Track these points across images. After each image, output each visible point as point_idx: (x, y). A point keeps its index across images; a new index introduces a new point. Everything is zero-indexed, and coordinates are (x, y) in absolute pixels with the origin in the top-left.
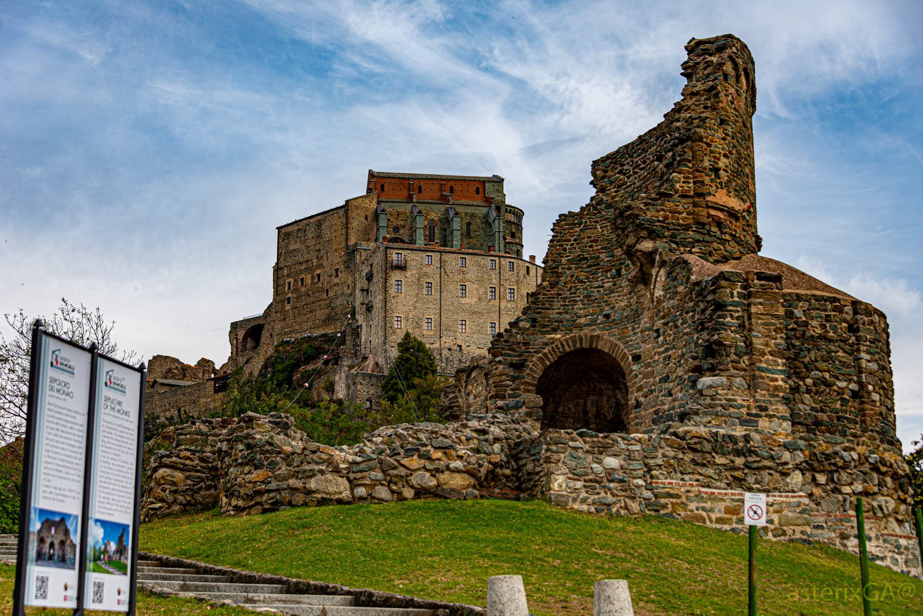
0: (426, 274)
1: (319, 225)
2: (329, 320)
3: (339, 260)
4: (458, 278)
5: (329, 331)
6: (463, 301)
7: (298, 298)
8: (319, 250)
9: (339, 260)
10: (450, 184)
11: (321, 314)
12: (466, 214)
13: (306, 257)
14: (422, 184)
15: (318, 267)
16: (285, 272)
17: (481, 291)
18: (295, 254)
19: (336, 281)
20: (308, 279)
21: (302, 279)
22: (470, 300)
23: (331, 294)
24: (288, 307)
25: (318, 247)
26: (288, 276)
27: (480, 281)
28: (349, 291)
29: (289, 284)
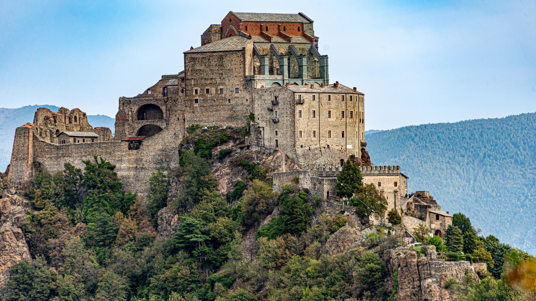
0: (313, 106)
1: (221, 58)
2: (231, 118)
3: (238, 83)
4: (327, 107)
5: (233, 125)
6: (330, 120)
7: (205, 100)
8: (222, 74)
9: (238, 83)
10: (284, 25)
11: (224, 113)
12: (300, 49)
13: (211, 76)
14: (268, 25)
15: (223, 84)
16: (193, 82)
17: (338, 114)
18: (201, 72)
19: (237, 95)
20: (213, 90)
21: (208, 91)
22: (333, 119)
23: (232, 102)
24: (196, 105)
25: (221, 72)
27: (337, 108)
28: (248, 103)
29: (196, 91)
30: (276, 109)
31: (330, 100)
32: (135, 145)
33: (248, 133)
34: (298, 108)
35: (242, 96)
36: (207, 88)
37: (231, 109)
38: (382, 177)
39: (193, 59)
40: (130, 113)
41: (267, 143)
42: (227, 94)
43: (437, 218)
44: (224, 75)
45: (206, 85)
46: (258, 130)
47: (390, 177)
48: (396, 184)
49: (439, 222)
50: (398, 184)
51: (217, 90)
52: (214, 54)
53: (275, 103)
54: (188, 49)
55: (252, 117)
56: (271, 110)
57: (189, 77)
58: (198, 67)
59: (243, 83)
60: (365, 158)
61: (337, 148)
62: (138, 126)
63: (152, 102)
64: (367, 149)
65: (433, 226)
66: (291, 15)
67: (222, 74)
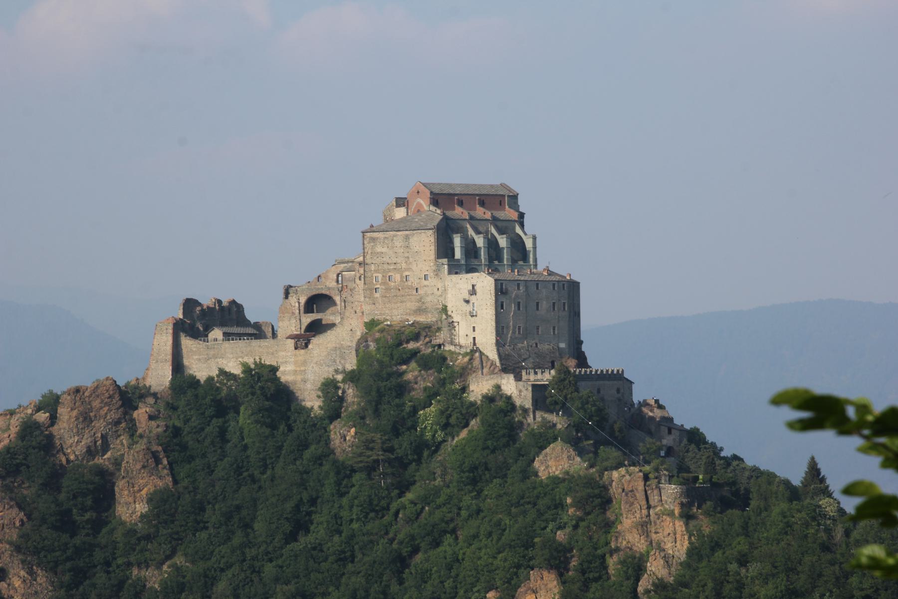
1: (407, 238)
2: (420, 311)
5: (422, 319)
6: (538, 313)
7: (388, 289)
8: (408, 257)
11: (412, 305)
13: (394, 260)
14: (463, 198)
15: (409, 269)
16: (373, 267)
19: (426, 283)
20: (397, 277)
23: (420, 292)
25: (407, 255)
26: (376, 271)
28: (439, 293)
30: (473, 299)
31: (537, 288)
32: (302, 341)
33: (439, 329)
34: (502, 298)
35: (432, 284)
36: (390, 274)
37: (420, 300)
38: (601, 382)
39: (373, 240)
40: (297, 305)
41: (462, 341)
42: (413, 281)
43: (670, 432)
44: (411, 259)
45: (389, 270)
46: (452, 326)
47: (611, 383)
48: (618, 391)
49: (671, 437)
50: (622, 391)
51: (402, 277)
52: (399, 233)
53: (473, 292)
54: (367, 227)
55: (445, 309)
56: (467, 302)
57: (368, 261)
58: (379, 249)
59: (434, 268)
60: (582, 361)
61: (547, 347)
62: (307, 319)
63: (324, 292)
64: (584, 348)
65: (665, 442)
66: (492, 186)
67: (408, 257)
